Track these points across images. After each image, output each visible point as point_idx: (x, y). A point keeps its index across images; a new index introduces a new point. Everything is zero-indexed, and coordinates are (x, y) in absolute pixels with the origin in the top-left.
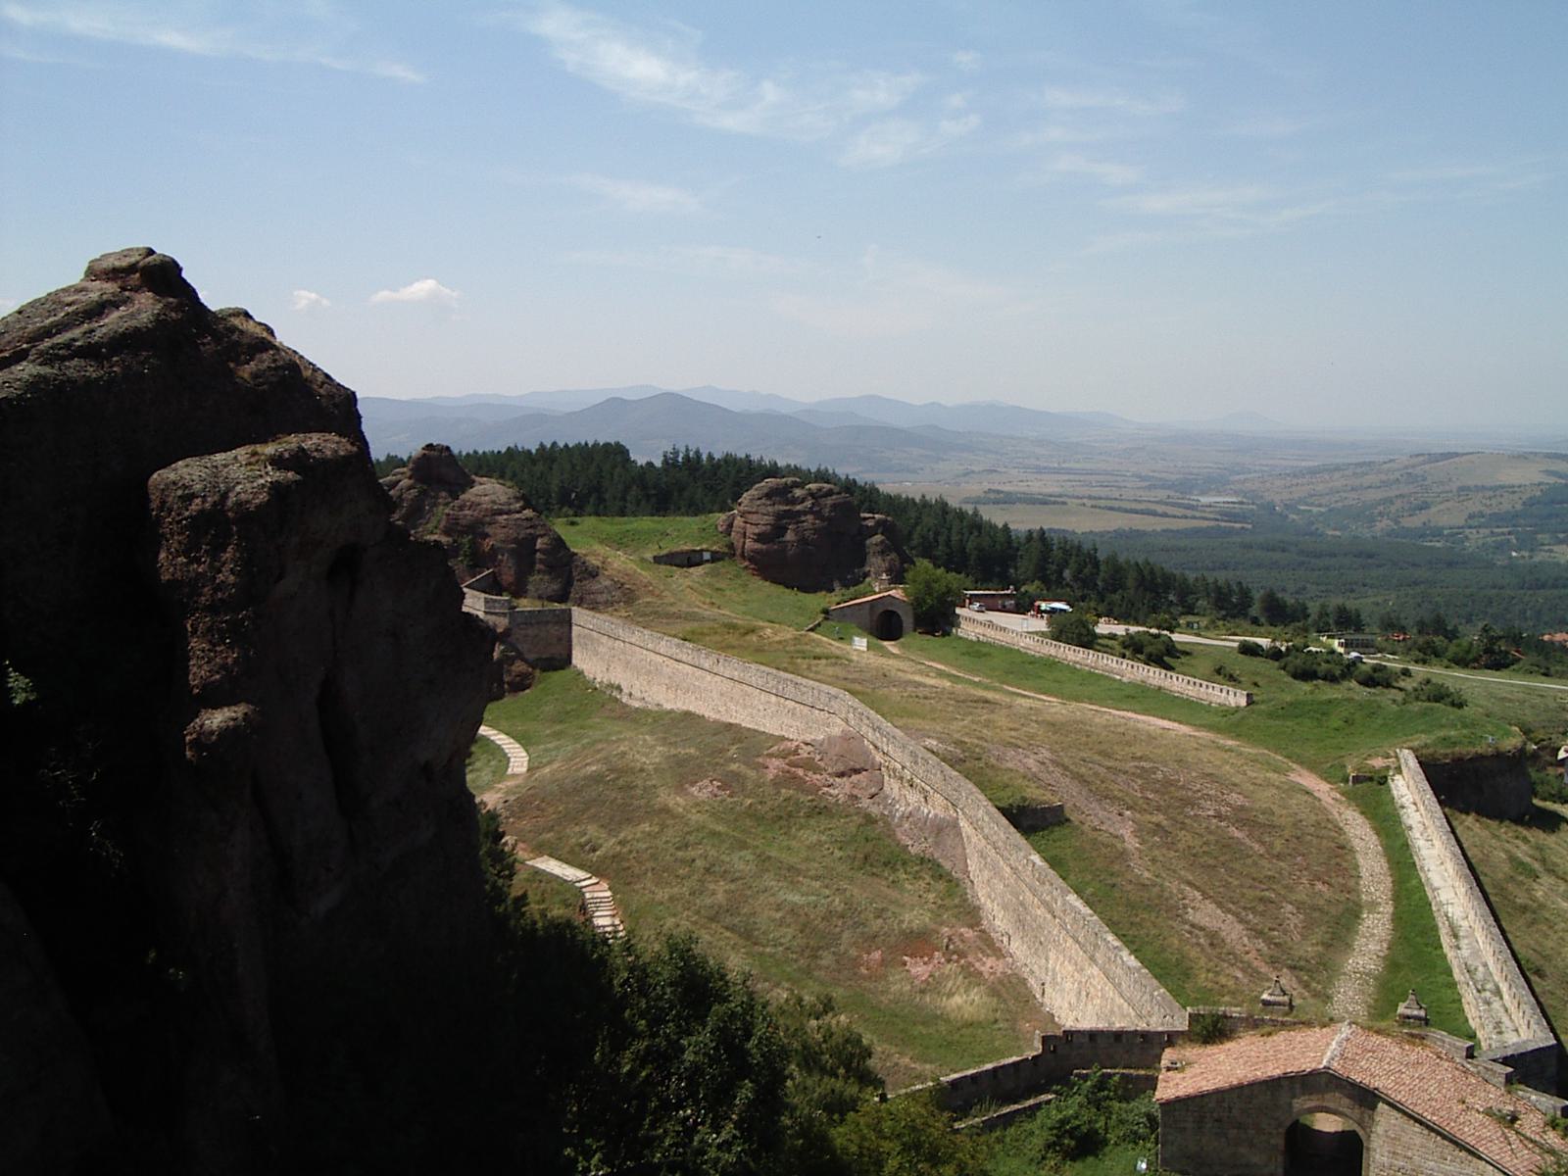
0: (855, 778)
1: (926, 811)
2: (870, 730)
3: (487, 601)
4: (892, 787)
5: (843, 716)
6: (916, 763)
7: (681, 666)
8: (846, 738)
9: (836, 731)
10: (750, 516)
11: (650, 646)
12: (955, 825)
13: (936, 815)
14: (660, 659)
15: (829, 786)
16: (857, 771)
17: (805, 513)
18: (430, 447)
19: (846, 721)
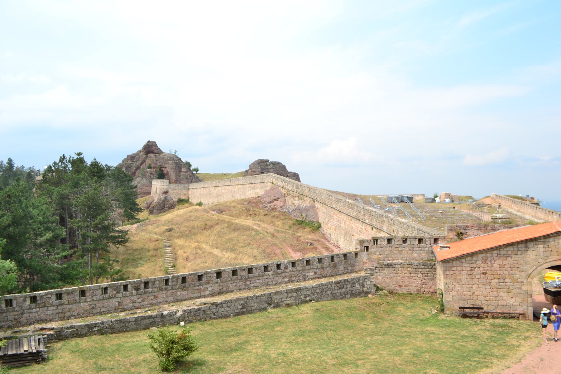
0: (275, 202)
1: (302, 206)
2: (281, 183)
3: (161, 182)
4: (289, 200)
5: (271, 181)
6: (298, 188)
7: (220, 188)
8: (272, 189)
9: (269, 188)
10: (253, 169)
11: (211, 186)
12: (313, 207)
13: (306, 206)
14: (213, 189)
15: (265, 207)
16: (275, 200)
17: (270, 169)
18: (149, 142)
19: (272, 183)
